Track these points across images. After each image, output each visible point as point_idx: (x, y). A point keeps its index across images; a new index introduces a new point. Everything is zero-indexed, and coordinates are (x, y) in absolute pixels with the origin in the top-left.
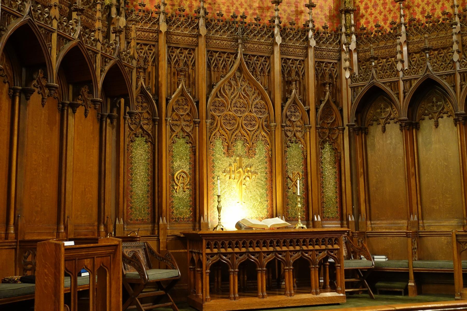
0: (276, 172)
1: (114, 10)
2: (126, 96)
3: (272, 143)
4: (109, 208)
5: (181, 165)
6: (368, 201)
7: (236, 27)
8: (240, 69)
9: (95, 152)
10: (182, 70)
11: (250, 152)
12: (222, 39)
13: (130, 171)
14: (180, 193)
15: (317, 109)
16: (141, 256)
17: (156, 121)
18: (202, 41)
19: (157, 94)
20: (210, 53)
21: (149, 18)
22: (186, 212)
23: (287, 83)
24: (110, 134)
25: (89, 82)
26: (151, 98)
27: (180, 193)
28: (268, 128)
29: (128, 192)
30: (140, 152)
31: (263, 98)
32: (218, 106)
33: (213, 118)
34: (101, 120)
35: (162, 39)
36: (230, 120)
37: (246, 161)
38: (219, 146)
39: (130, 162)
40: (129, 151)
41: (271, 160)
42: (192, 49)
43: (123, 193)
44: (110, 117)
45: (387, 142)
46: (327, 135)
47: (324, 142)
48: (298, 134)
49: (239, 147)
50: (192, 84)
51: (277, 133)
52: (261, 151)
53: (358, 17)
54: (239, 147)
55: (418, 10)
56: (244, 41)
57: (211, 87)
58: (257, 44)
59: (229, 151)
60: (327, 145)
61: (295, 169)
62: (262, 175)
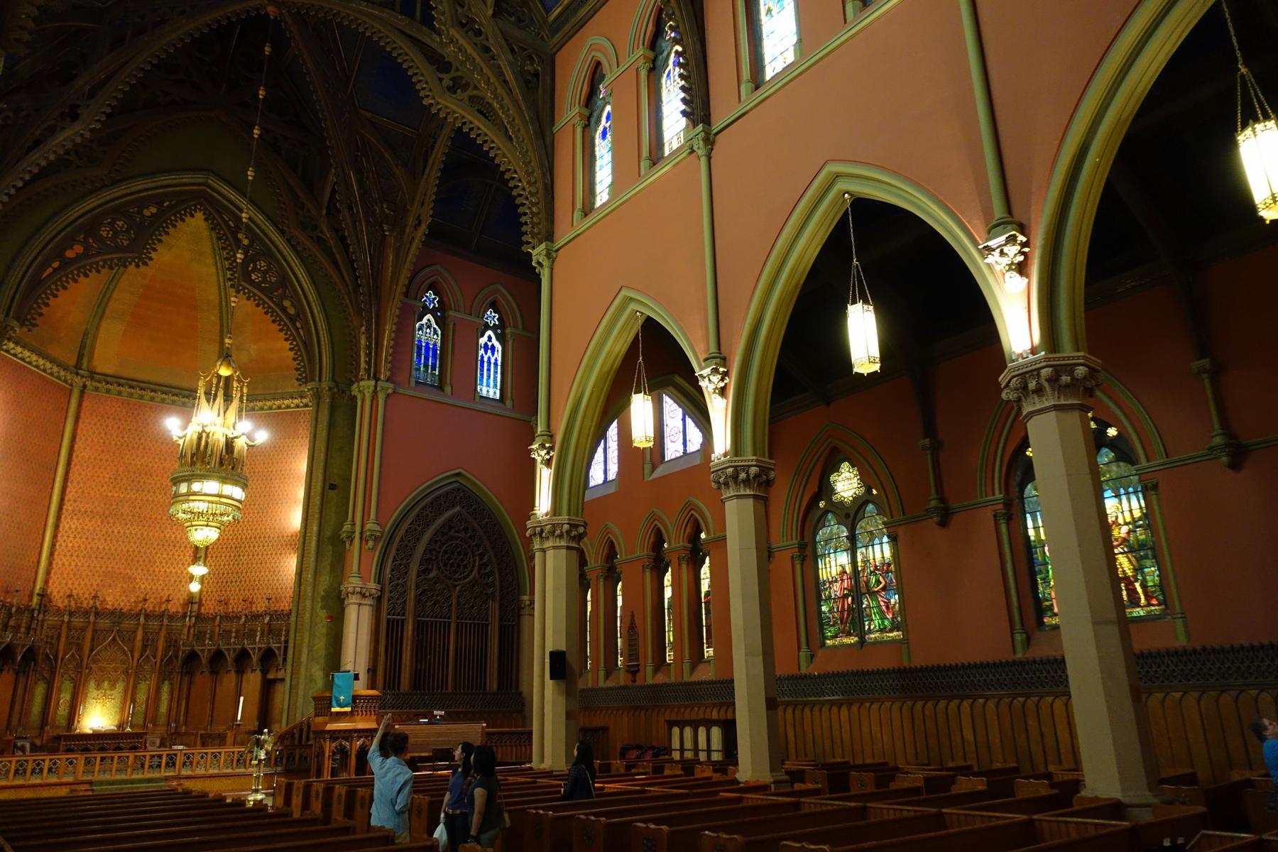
0: (130, 697)
2: (35, 661)
3: (128, 682)
4: (15, 721)
5: (65, 697)
8: (114, 639)
11: (113, 687)
12: (104, 623)
13: (31, 700)
16: (28, 746)
17: (53, 673)
19: (56, 657)
21: (59, 611)
22: (63, 722)
23: (144, 647)
24: (22, 680)
25: (14, 660)
27: (63, 711)
28: (126, 672)
29: (28, 713)
30: (40, 690)
32: (94, 661)
35: (65, 626)
36: (101, 669)
38: (92, 684)
39: (32, 694)
41: (126, 692)
42: (83, 629)
43: (25, 713)
45: (203, 679)
46: (164, 676)
50: (80, 649)
51: (133, 677)
52: (120, 686)
57: (92, 650)
58: (128, 624)
59: (98, 687)
61: (141, 697)
62: (118, 701)
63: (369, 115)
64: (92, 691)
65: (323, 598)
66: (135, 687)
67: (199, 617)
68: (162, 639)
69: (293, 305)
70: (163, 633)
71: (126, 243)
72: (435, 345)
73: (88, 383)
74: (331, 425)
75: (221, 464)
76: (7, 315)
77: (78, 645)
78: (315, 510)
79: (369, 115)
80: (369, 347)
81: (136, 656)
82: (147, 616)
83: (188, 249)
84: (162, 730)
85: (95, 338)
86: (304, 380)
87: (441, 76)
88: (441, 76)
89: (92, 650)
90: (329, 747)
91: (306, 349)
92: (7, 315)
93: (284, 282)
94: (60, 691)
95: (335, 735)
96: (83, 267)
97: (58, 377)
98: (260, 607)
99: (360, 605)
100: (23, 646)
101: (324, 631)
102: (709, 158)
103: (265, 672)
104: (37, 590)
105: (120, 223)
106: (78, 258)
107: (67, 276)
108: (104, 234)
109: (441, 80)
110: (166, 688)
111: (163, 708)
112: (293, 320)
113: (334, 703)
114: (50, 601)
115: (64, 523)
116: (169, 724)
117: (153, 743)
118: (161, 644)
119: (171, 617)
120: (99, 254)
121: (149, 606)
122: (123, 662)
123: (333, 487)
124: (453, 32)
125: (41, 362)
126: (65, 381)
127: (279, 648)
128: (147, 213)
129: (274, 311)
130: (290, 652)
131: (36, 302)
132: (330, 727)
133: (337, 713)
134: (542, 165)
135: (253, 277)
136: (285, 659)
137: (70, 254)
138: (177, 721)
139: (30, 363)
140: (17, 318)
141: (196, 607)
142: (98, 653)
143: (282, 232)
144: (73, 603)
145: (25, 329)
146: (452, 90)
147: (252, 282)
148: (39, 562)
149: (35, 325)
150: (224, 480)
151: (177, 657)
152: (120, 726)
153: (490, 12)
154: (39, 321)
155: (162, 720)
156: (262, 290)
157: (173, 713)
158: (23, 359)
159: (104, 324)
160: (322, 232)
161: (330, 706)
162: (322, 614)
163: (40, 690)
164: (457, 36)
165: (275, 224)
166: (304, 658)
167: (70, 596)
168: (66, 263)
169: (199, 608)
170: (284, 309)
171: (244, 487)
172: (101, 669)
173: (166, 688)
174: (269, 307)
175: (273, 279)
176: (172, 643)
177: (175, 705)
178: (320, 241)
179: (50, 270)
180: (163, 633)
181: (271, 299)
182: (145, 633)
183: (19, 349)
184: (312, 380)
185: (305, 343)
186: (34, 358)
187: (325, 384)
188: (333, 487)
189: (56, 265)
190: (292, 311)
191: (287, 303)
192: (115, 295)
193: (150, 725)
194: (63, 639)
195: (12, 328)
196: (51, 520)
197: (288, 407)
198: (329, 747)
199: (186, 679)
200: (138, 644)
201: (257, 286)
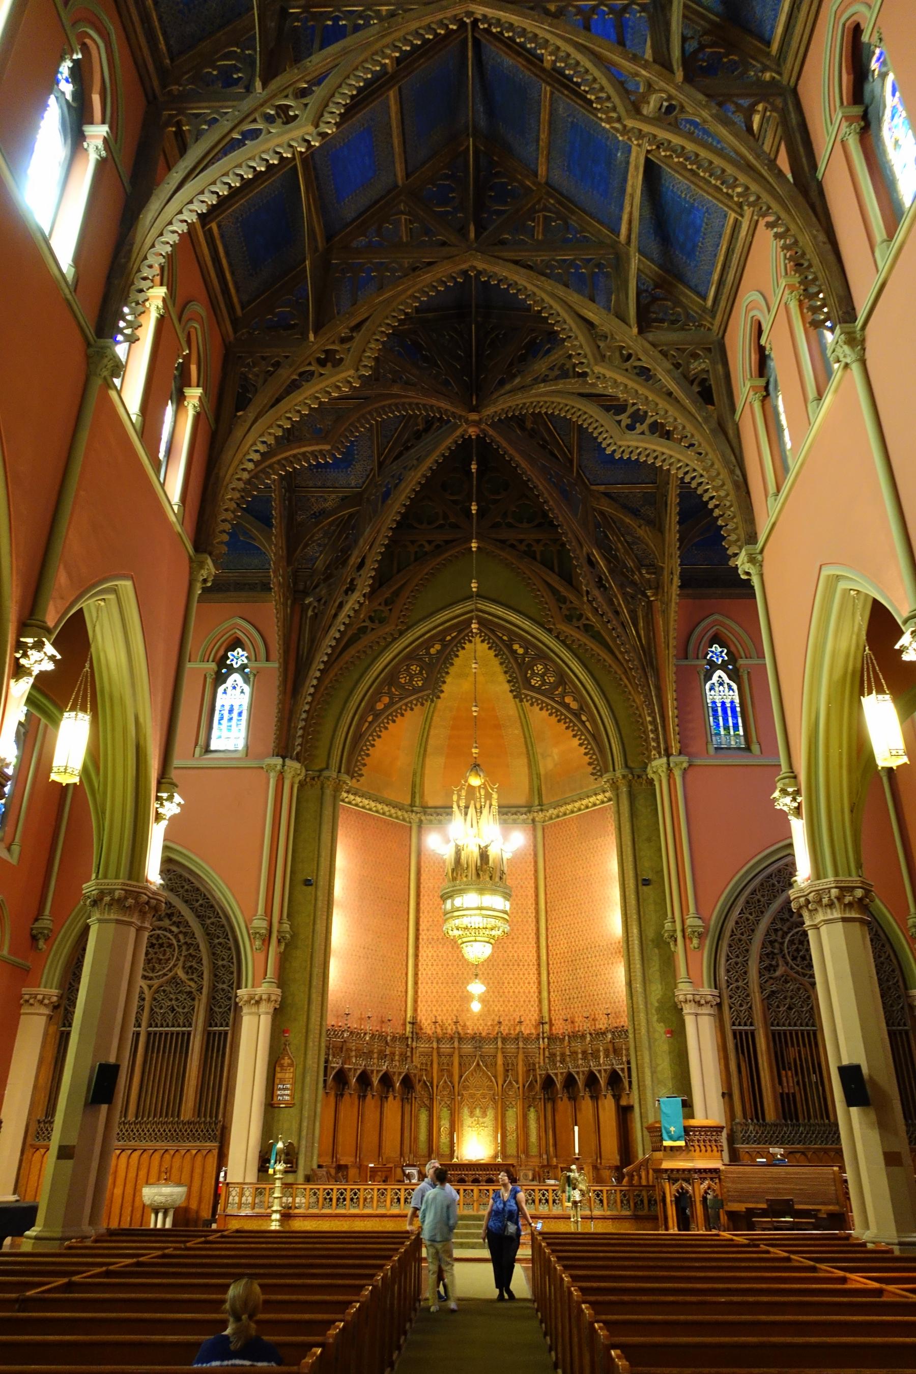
0: (501, 1126)
1: (410, 1040)
3: (496, 1109)
4: (406, 1149)
5: (445, 1124)
6: (555, 1145)
7: (478, 1040)
8: (478, 1065)
9: (400, 1118)
10: (446, 1070)
11: (484, 1114)
12: (468, 1048)
14: (444, 1139)
15: (524, 1086)
17: (431, 1099)
18: (457, 1052)
19: (432, 1083)
20: (461, 1056)
21: (429, 1039)
24: (407, 1108)
26: (428, 1087)
27: (444, 1139)
29: (416, 1139)
30: (423, 1117)
31: (491, 1081)
32: (466, 1088)
33: (463, 1095)
34: (402, 1100)
37: (481, 1120)
38: (466, 1111)
40: (417, 1117)
41: (496, 1119)
42: (451, 1055)
44: (407, 1099)
47: (530, 1106)
48: (514, 1103)
49: (478, 1112)
50: (451, 1076)
52: (490, 1113)
53: (551, 1025)
54: (478, 1112)
55: (577, 1025)
56: (480, 1047)
57: (461, 1077)
58: (488, 1048)
59: (472, 1114)
60: (532, 1109)
61: (511, 1125)
63: (602, 488)
64: (468, 1121)
65: (658, 1010)
66: (503, 1116)
67: (552, 1038)
68: (521, 1063)
69: (575, 699)
70: (521, 1056)
71: (420, 684)
72: (732, 702)
73: (423, 818)
74: (633, 814)
75: (478, 875)
76: (339, 772)
77: (448, 1071)
78: (633, 911)
79: (602, 488)
80: (654, 722)
81: (500, 1083)
82: (504, 1040)
83: (477, 673)
84: (535, 1162)
85: (422, 775)
86: (598, 773)
87: (618, 418)
88: (618, 418)
89: (461, 1077)
90: (670, 1190)
91: (595, 742)
92: (339, 772)
93: (562, 679)
94: (439, 1118)
95: (674, 1175)
96: (391, 714)
97: (397, 818)
98: (602, 1025)
99: (697, 1015)
100: (400, 1074)
101: (666, 1047)
102: (863, 362)
103: (617, 1098)
104: (408, 1020)
105: (413, 667)
106: (387, 707)
107: (379, 726)
108: (403, 681)
109: (619, 422)
110: (532, 1115)
111: (533, 1138)
112: (577, 715)
113: (665, 1136)
114: (421, 1029)
115: (422, 953)
116: (541, 1156)
117: (526, 1175)
118: (521, 1069)
119: (527, 1039)
120: (401, 699)
121: (505, 1030)
122: (490, 1088)
123: (646, 882)
124: (597, 369)
125: (380, 807)
126: (404, 820)
127: (622, 1070)
128: (433, 651)
129: (557, 710)
130: (634, 1074)
131: (360, 755)
132: (666, 1165)
133: (672, 1148)
134: (726, 463)
135: (533, 682)
136: (630, 1083)
137: (380, 706)
138: (547, 1153)
139: (370, 809)
140: (348, 773)
141: (547, 1027)
142: (466, 1080)
143: (550, 631)
144: (439, 1030)
145: (354, 780)
146: (631, 427)
147: (532, 688)
148: (406, 992)
149: (361, 775)
150: (481, 891)
151: (536, 1081)
152: (496, 1156)
153: (635, 330)
154: (364, 771)
155: (534, 1151)
156: (542, 693)
157: (543, 1142)
158: (363, 807)
159: (427, 760)
160: (587, 619)
161: (662, 1140)
162: (660, 1029)
163: (423, 1117)
164: (602, 371)
165: (541, 625)
166: (648, 1082)
167: (435, 1022)
168: (377, 716)
169: (551, 1029)
170: (567, 706)
171: (507, 896)
172: (472, 1096)
173: (532, 1115)
174: (553, 707)
175: (552, 680)
176: (530, 1068)
177: (543, 1134)
178: (587, 628)
179: (367, 724)
180: (521, 1056)
181: (553, 699)
182: (505, 1057)
183: (358, 799)
184: (607, 771)
185: (593, 736)
186: (373, 804)
187: (619, 773)
188: (646, 882)
189: (370, 719)
190: (574, 705)
191: (568, 700)
192: (432, 732)
193: (523, 1156)
194: (435, 1066)
195: (345, 783)
196: (411, 951)
197: (595, 805)
198: (670, 1190)
199: (549, 1106)
200: (500, 1069)
201: (537, 690)
